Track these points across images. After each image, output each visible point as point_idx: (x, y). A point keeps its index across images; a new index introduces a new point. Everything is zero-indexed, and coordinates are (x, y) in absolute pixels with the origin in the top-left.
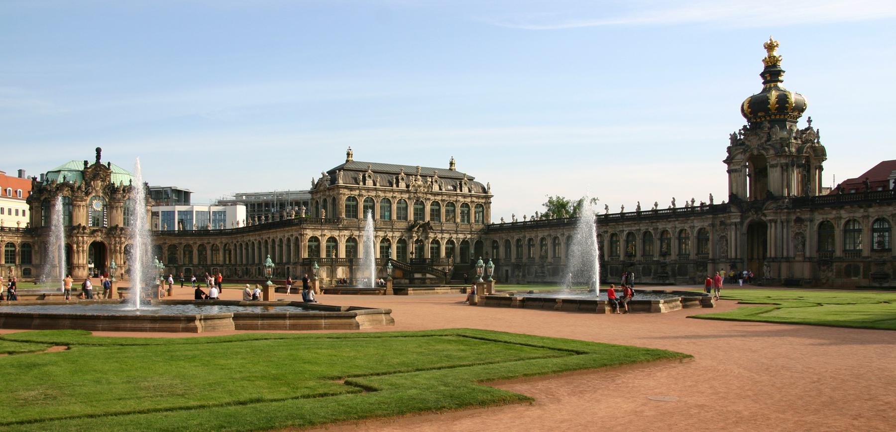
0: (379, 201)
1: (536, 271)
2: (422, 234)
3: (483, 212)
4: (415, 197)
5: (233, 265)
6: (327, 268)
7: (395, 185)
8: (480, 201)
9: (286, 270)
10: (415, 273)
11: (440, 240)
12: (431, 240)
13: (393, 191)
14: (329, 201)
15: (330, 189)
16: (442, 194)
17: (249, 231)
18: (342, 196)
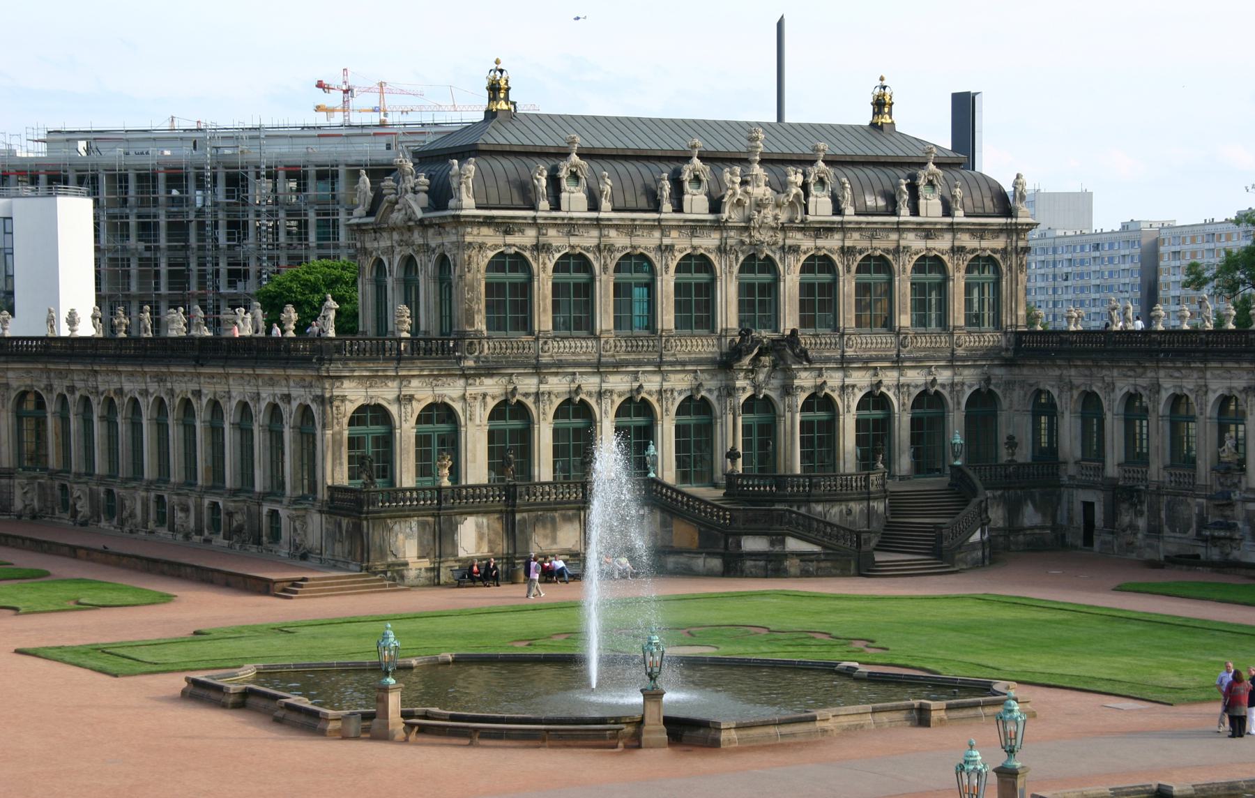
0: (612, 266)
1: (1200, 515)
2: (769, 376)
3: (997, 284)
4: (742, 243)
5: (53, 474)
6: (422, 525)
7: (667, 206)
8: (985, 244)
9: (265, 519)
10: (746, 534)
11: (835, 395)
12: (801, 398)
13: (659, 226)
14: (426, 268)
15: (431, 225)
16: (843, 229)
17: (119, 358)
18: (474, 253)
